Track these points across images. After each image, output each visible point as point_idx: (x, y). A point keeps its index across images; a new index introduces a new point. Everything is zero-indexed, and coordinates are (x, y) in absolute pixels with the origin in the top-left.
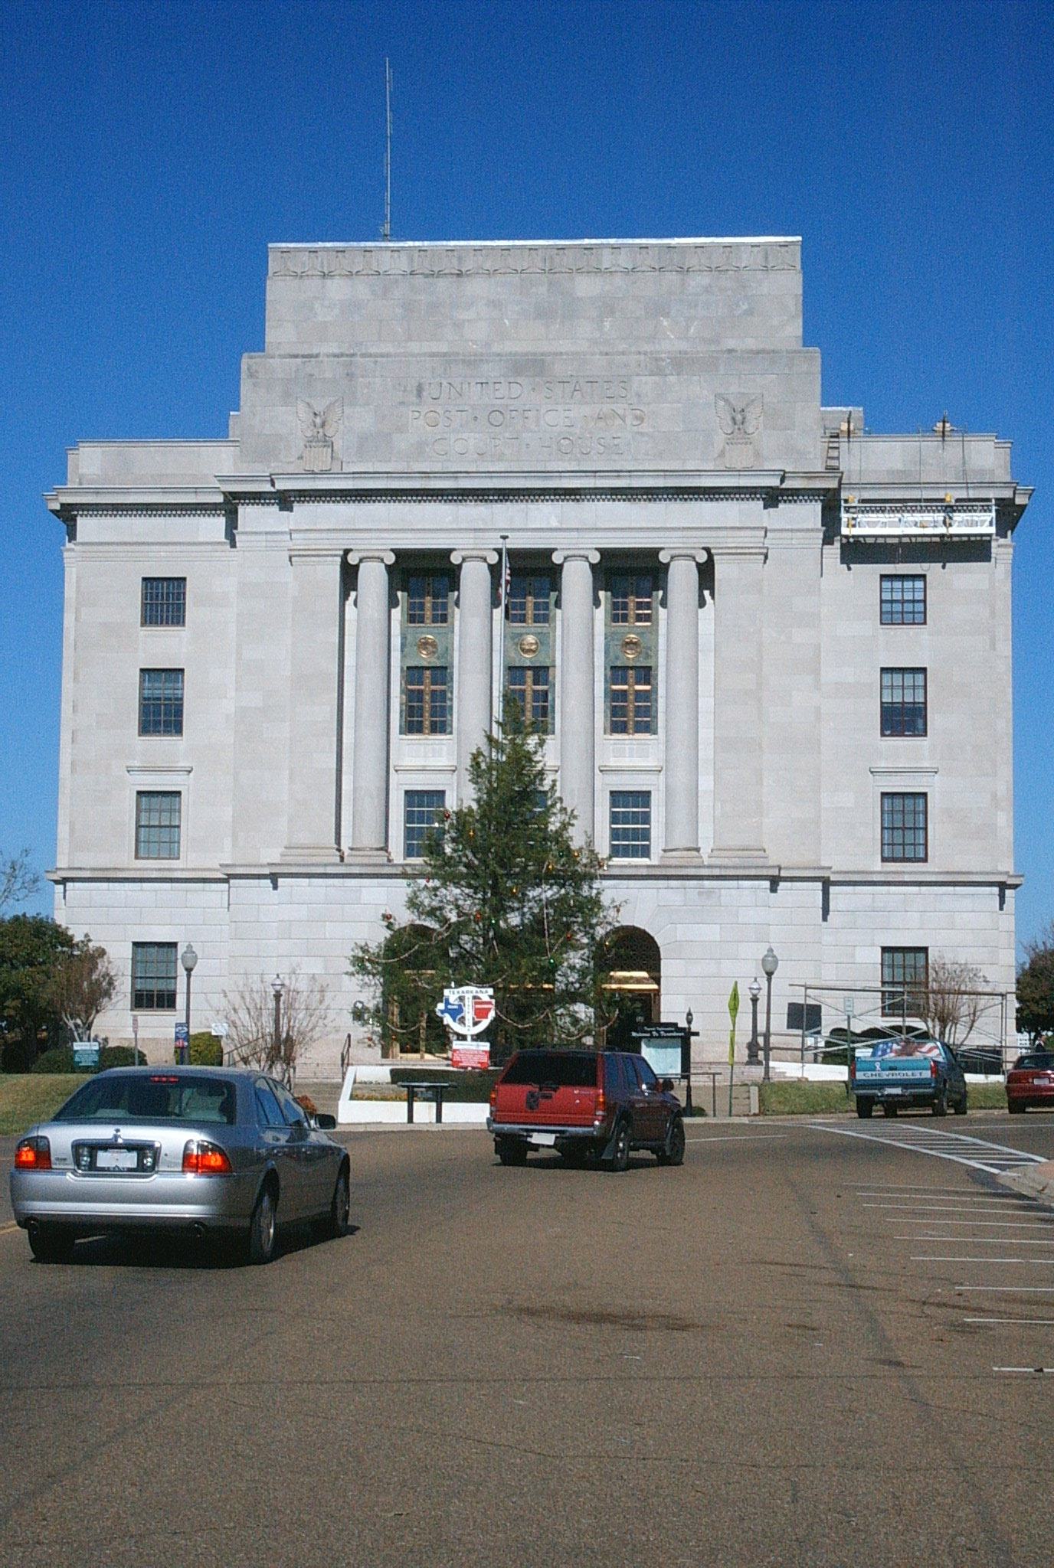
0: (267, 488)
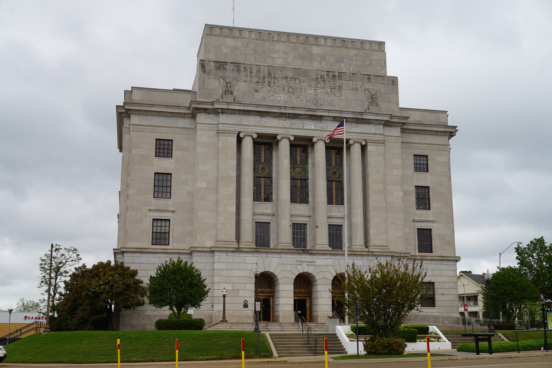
0: (210, 107)
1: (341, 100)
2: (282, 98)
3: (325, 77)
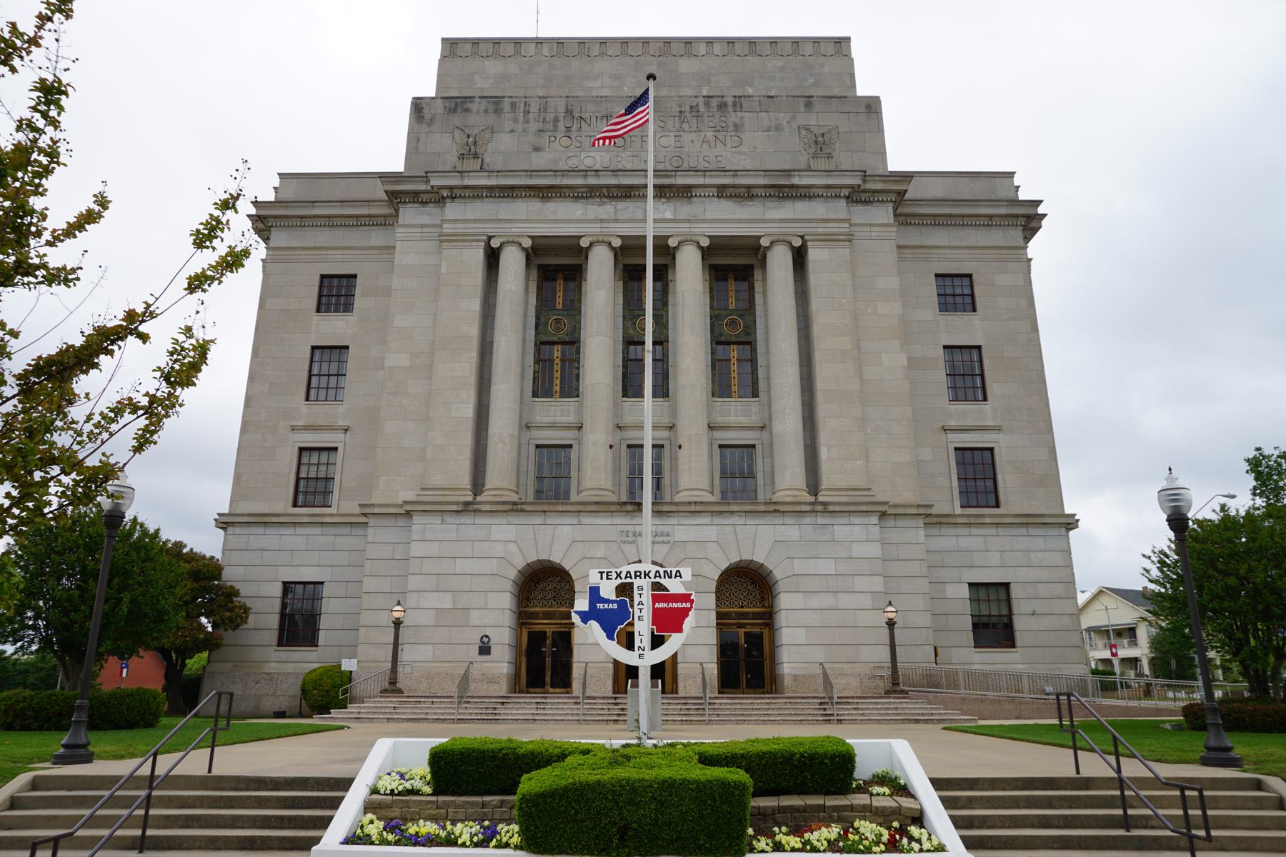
0: (423, 187)
1: (741, 153)
2: (598, 159)
3: (702, 108)
